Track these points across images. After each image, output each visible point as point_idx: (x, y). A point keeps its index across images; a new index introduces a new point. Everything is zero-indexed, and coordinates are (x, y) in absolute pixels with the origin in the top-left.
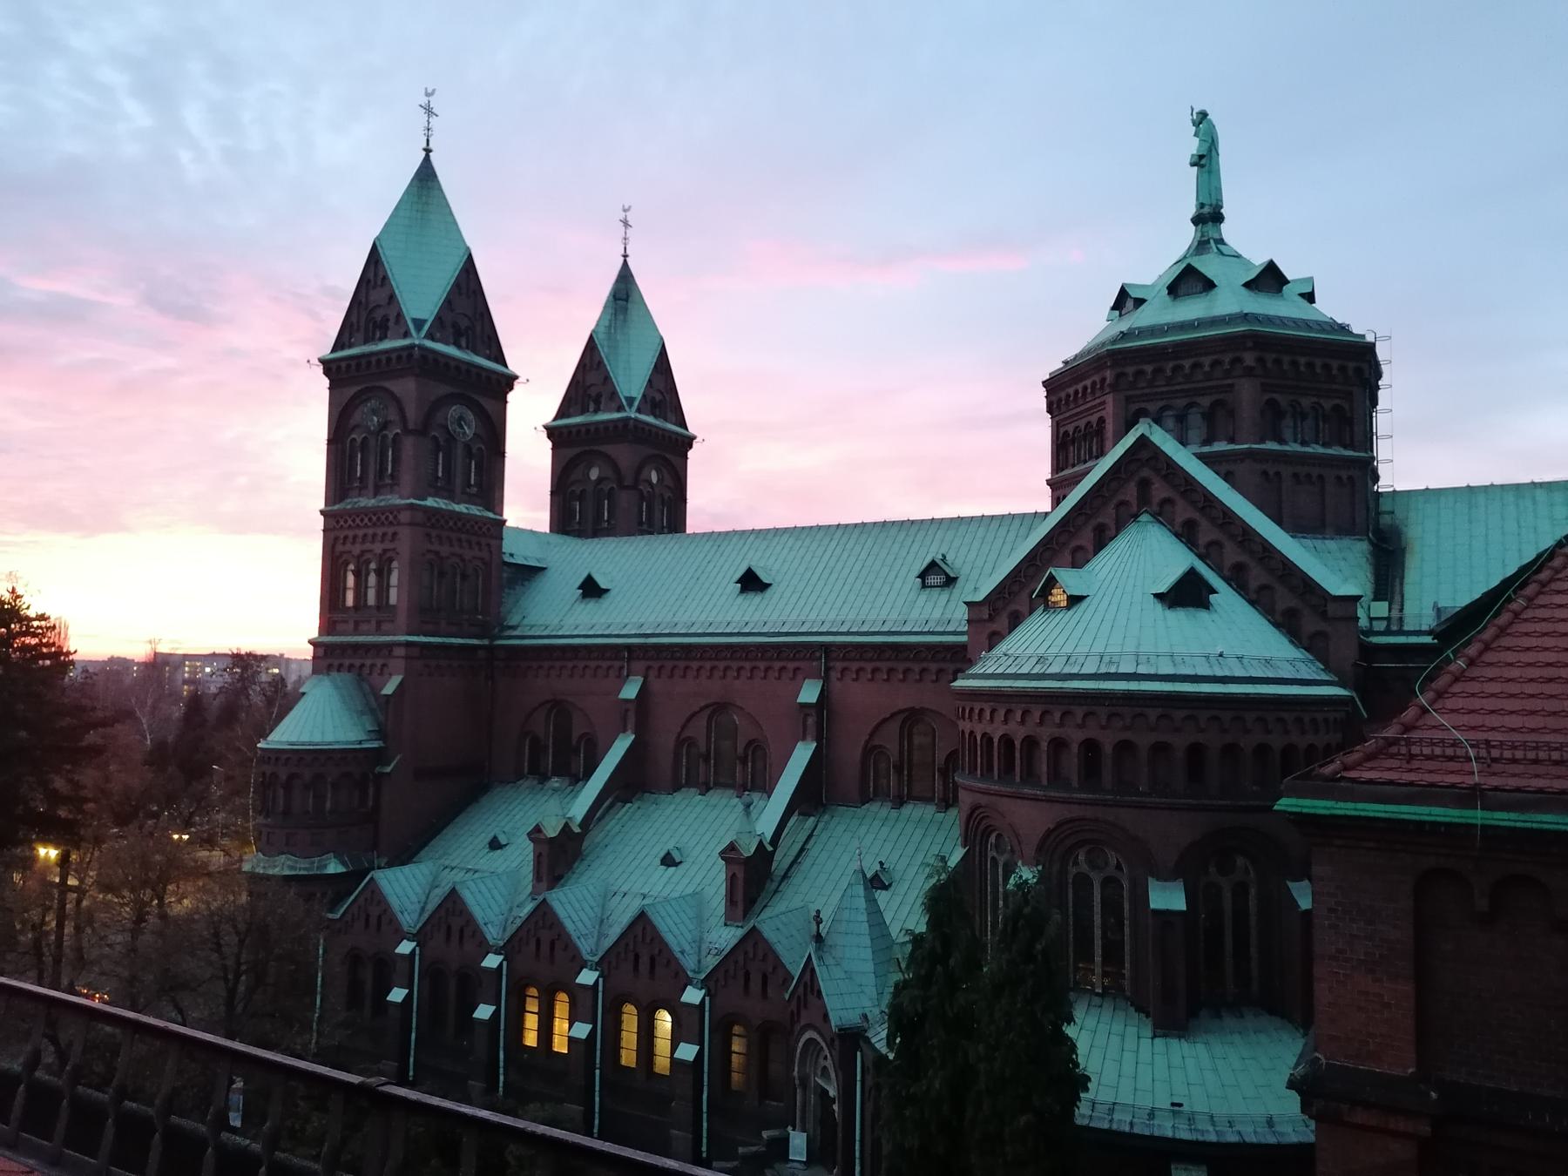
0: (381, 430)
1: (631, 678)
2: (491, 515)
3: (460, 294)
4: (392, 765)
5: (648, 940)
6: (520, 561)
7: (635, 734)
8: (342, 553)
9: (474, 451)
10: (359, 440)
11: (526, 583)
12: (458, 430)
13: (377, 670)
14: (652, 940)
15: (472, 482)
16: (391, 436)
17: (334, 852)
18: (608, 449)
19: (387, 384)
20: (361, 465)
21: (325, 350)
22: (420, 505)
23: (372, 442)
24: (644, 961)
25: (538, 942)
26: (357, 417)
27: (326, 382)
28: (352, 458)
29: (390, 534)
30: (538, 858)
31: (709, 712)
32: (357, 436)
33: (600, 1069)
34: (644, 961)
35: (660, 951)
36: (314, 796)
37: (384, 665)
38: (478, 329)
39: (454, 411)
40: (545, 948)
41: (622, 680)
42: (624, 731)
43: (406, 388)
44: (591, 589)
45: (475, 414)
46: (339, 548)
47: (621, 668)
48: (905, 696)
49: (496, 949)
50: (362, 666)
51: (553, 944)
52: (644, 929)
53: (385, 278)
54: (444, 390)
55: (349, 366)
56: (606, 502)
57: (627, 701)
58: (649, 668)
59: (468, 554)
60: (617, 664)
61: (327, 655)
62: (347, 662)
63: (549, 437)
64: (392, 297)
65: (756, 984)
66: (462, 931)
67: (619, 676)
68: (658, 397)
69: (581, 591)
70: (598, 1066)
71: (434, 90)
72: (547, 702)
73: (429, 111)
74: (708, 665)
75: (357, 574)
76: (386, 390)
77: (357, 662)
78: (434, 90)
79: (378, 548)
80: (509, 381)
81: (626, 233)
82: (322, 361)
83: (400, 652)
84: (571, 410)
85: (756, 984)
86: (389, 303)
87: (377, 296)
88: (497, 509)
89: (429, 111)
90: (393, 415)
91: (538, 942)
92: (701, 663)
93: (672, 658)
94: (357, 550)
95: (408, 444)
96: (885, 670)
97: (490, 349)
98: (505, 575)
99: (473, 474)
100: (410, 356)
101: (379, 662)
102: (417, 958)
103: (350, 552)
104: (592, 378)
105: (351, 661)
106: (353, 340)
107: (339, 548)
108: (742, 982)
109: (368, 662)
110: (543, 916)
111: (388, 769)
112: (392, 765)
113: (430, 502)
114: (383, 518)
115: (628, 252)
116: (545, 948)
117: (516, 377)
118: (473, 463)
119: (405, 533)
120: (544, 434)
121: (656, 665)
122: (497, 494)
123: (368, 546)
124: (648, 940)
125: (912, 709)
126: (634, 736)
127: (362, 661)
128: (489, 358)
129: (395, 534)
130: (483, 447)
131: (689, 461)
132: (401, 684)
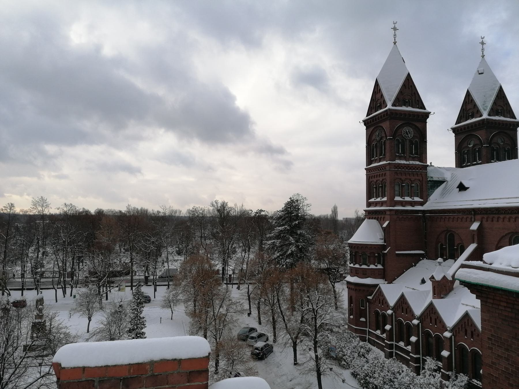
0: (380, 140)
2: (420, 163)
3: (406, 88)
4: (387, 250)
5: (470, 324)
6: (435, 179)
7: (478, 243)
8: (371, 182)
9: (414, 142)
10: (375, 145)
13: (382, 219)
14: (471, 325)
15: (414, 153)
16: (383, 142)
19: (381, 125)
20: (376, 152)
21: (364, 117)
22: (393, 163)
23: (378, 144)
24: (469, 332)
25: (431, 318)
26: (374, 137)
27: (365, 127)
28: (373, 149)
29: (384, 174)
30: (434, 288)
31: (510, 236)
32: (374, 143)
34: (469, 332)
35: (475, 330)
36: (363, 259)
37: (384, 218)
38: (414, 99)
39: (406, 129)
41: (472, 222)
42: (473, 243)
43: (386, 125)
44: (462, 188)
46: (371, 180)
47: (472, 218)
49: (417, 318)
50: (378, 218)
52: (468, 320)
53: (380, 90)
55: (373, 120)
56: (477, 153)
57: (473, 231)
58: (483, 218)
59: (413, 178)
60: (470, 216)
61: (370, 214)
62: (374, 216)
64: (382, 95)
66: (406, 309)
67: (471, 221)
68: (500, 108)
69: (458, 189)
71: (396, 22)
72: (444, 231)
73: (395, 29)
74: (508, 216)
75: (376, 188)
76: (382, 127)
77: (377, 217)
78: (396, 22)
80: (427, 115)
81: (483, 47)
82: (363, 121)
83: (388, 213)
84: (462, 120)
86: (381, 98)
87: (378, 96)
88: (424, 162)
89: (395, 29)
90: (384, 135)
91: (431, 318)
92: (510, 215)
93: (492, 214)
94: (375, 180)
95: (388, 143)
97: (419, 106)
98: (429, 185)
99: (414, 150)
100: (387, 114)
101: (383, 216)
102: (394, 316)
103: (373, 181)
104: (469, 106)
105: (375, 216)
106: (372, 112)
107: (371, 180)
109: (380, 216)
110: (431, 309)
111: (386, 252)
112: (387, 250)
113: (398, 161)
114: (382, 169)
115: (484, 54)
117: (430, 113)
118: (414, 146)
119: (388, 173)
120: (451, 132)
121: (485, 216)
122: (423, 156)
123: (378, 178)
124: (470, 324)
127: (378, 216)
128: (418, 108)
129: (385, 174)
130: (417, 140)
131: (518, 132)
132: (389, 223)
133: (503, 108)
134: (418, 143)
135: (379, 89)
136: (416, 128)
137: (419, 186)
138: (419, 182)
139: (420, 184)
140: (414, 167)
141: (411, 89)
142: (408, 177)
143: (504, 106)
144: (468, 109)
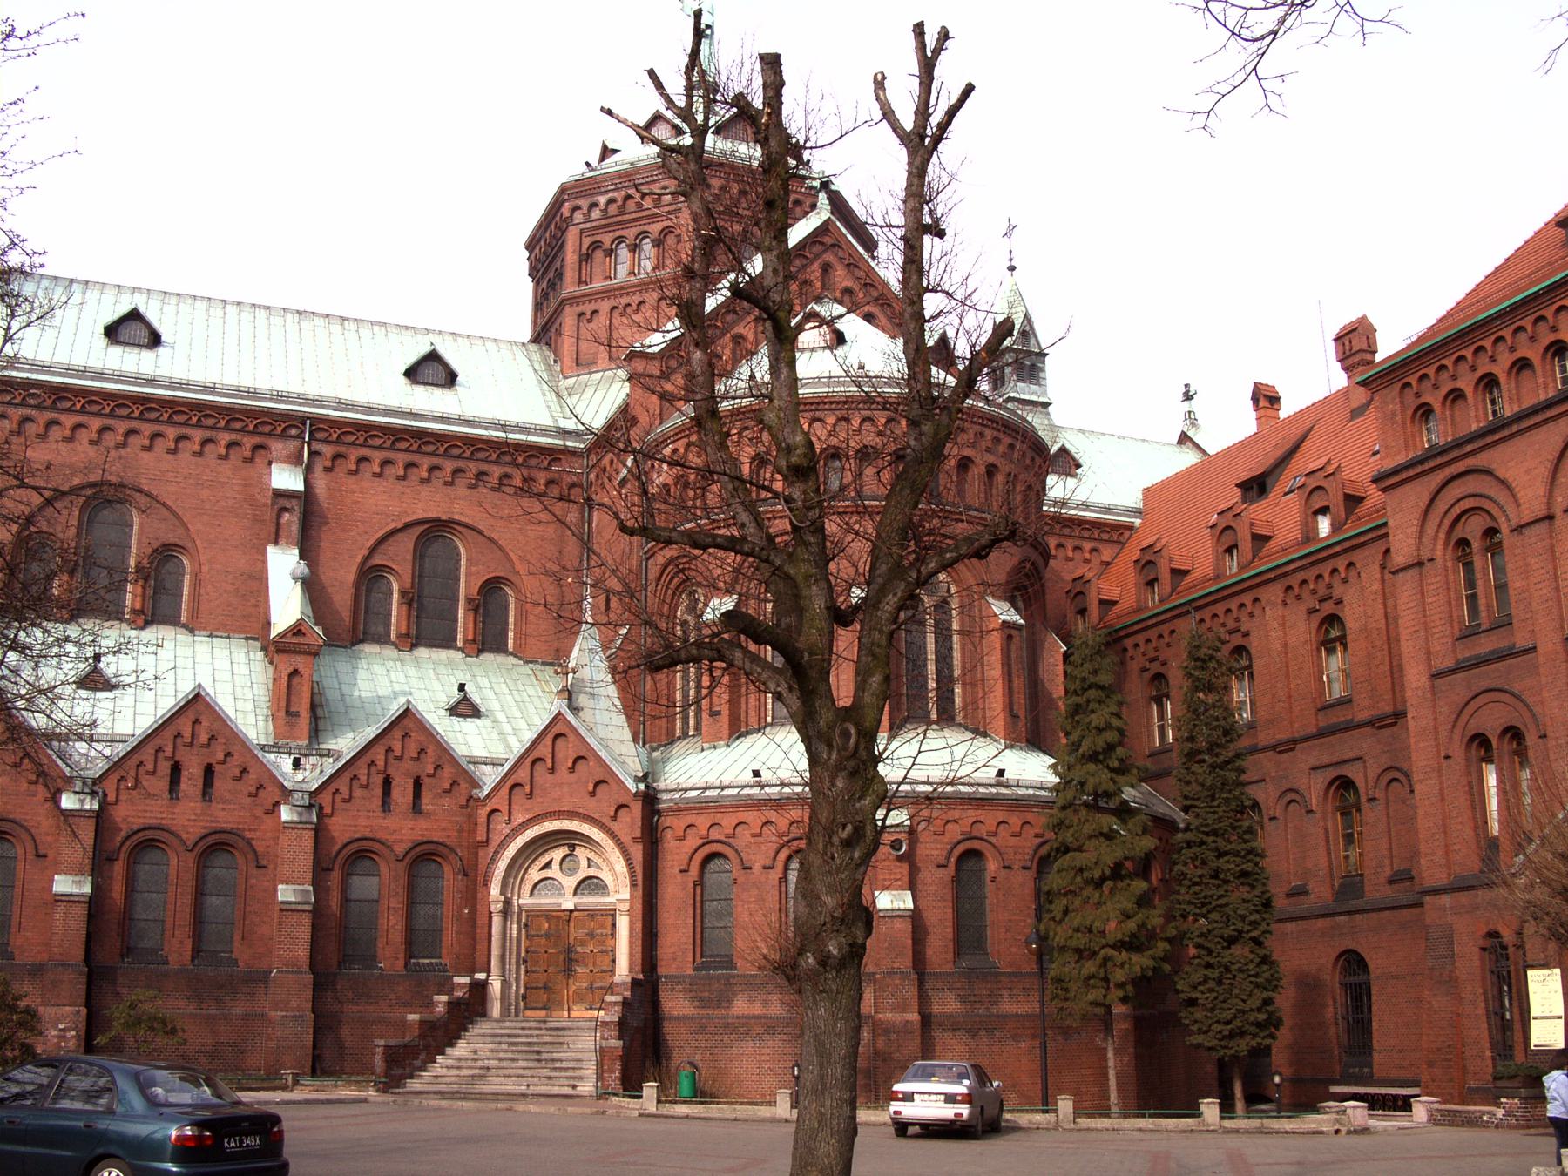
5: (204, 738)
35: (228, 754)
48: (429, 502)
65: (402, 794)
85: (402, 794)
96: (401, 464)
108: (378, 791)
125: (438, 520)
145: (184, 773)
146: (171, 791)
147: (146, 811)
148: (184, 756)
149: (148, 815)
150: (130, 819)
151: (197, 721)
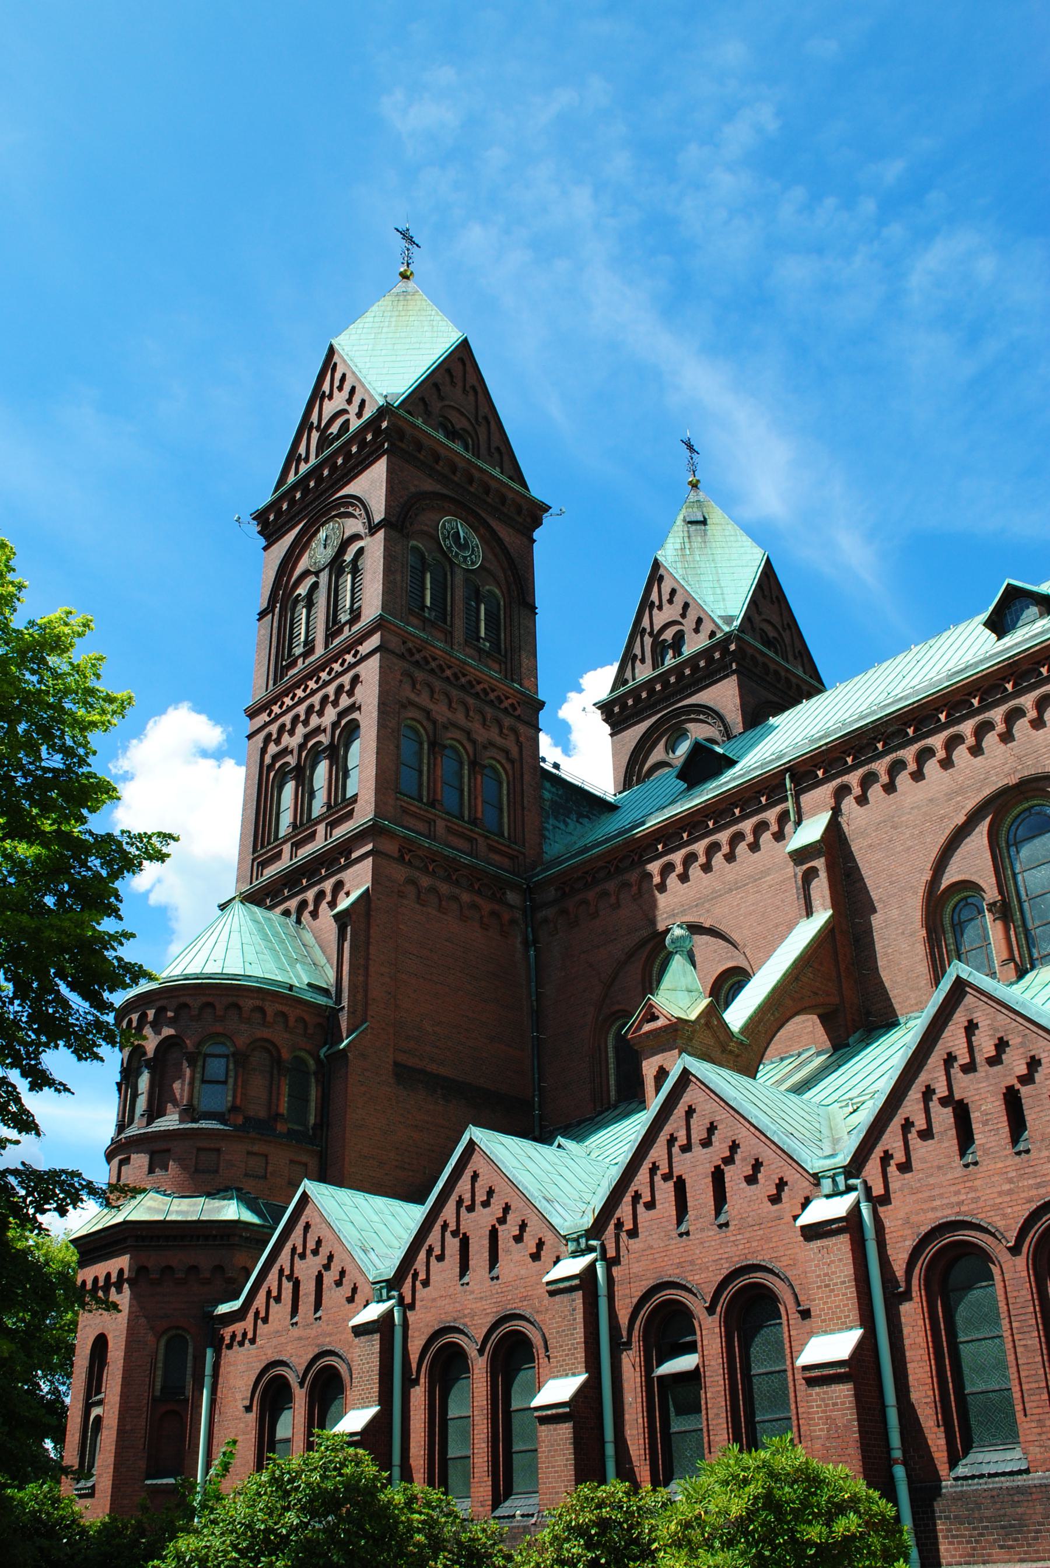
1: (804, 823)
8: (276, 757)
11: (585, 821)
12: (455, 549)
17: (239, 1190)
18: (703, 697)
33: (905, 1463)
38: (483, 438)
40: (700, 1194)
45: (481, 538)
51: (718, 1177)
54: (429, 485)
63: (606, 720)
70: (897, 1454)
79: (331, 714)
116: (700, 1194)
117: (546, 508)
118: (483, 607)
122: (525, 661)
126: (830, 912)
133: (780, 634)
134: (499, 604)
135: (338, 376)
136: (492, 539)
137: (505, 785)
138: (508, 766)
139: (510, 772)
140: (486, 686)
141: (471, 398)
142: (460, 717)
143: (784, 629)
144: (656, 628)
145: (974, 1115)
146: (962, 1154)
147: (932, 1198)
148: (965, 1087)
149: (937, 1203)
150: (914, 1219)
151: (971, 1028)
